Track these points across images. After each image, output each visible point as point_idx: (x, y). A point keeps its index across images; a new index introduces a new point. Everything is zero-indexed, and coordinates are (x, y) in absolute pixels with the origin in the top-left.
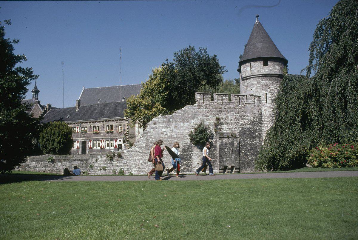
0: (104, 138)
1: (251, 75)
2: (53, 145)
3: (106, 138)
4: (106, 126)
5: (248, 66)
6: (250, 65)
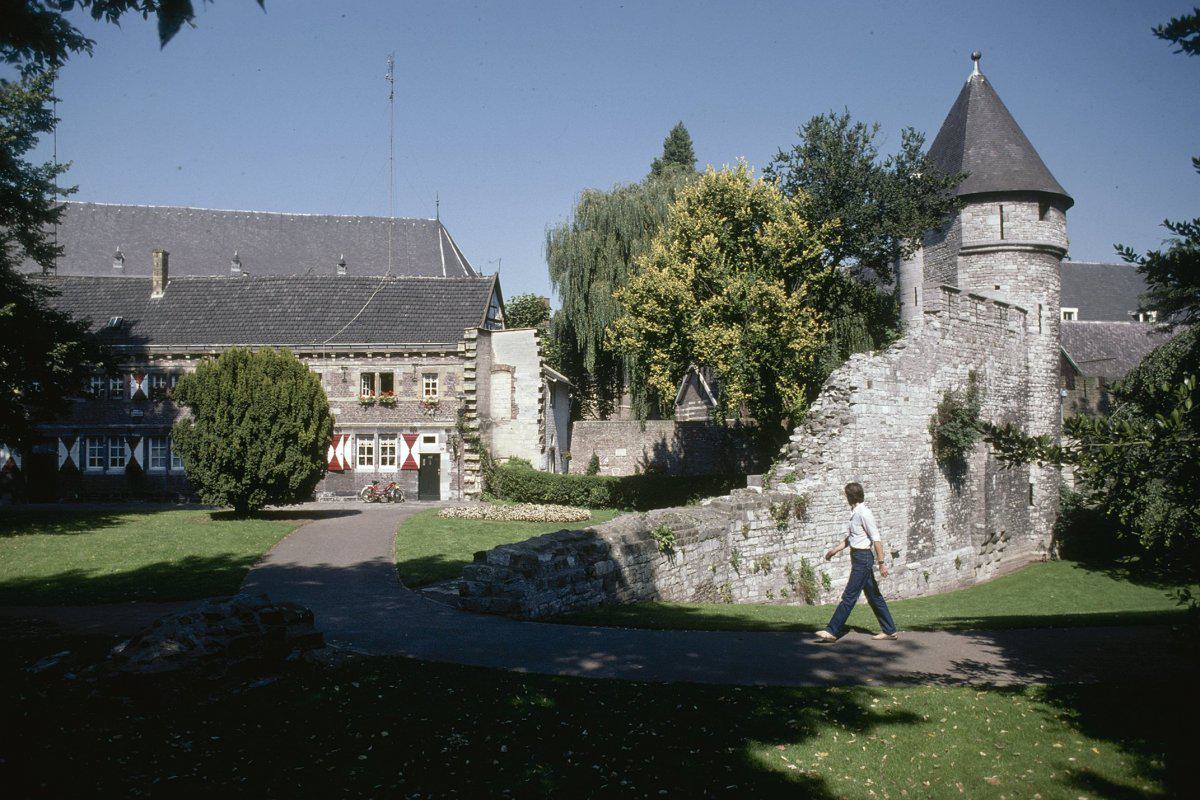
0: (350, 428)
1: (1003, 242)
2: (280, 459)
3: (357, 428)
4: (356, 376)
6: (999, 210)
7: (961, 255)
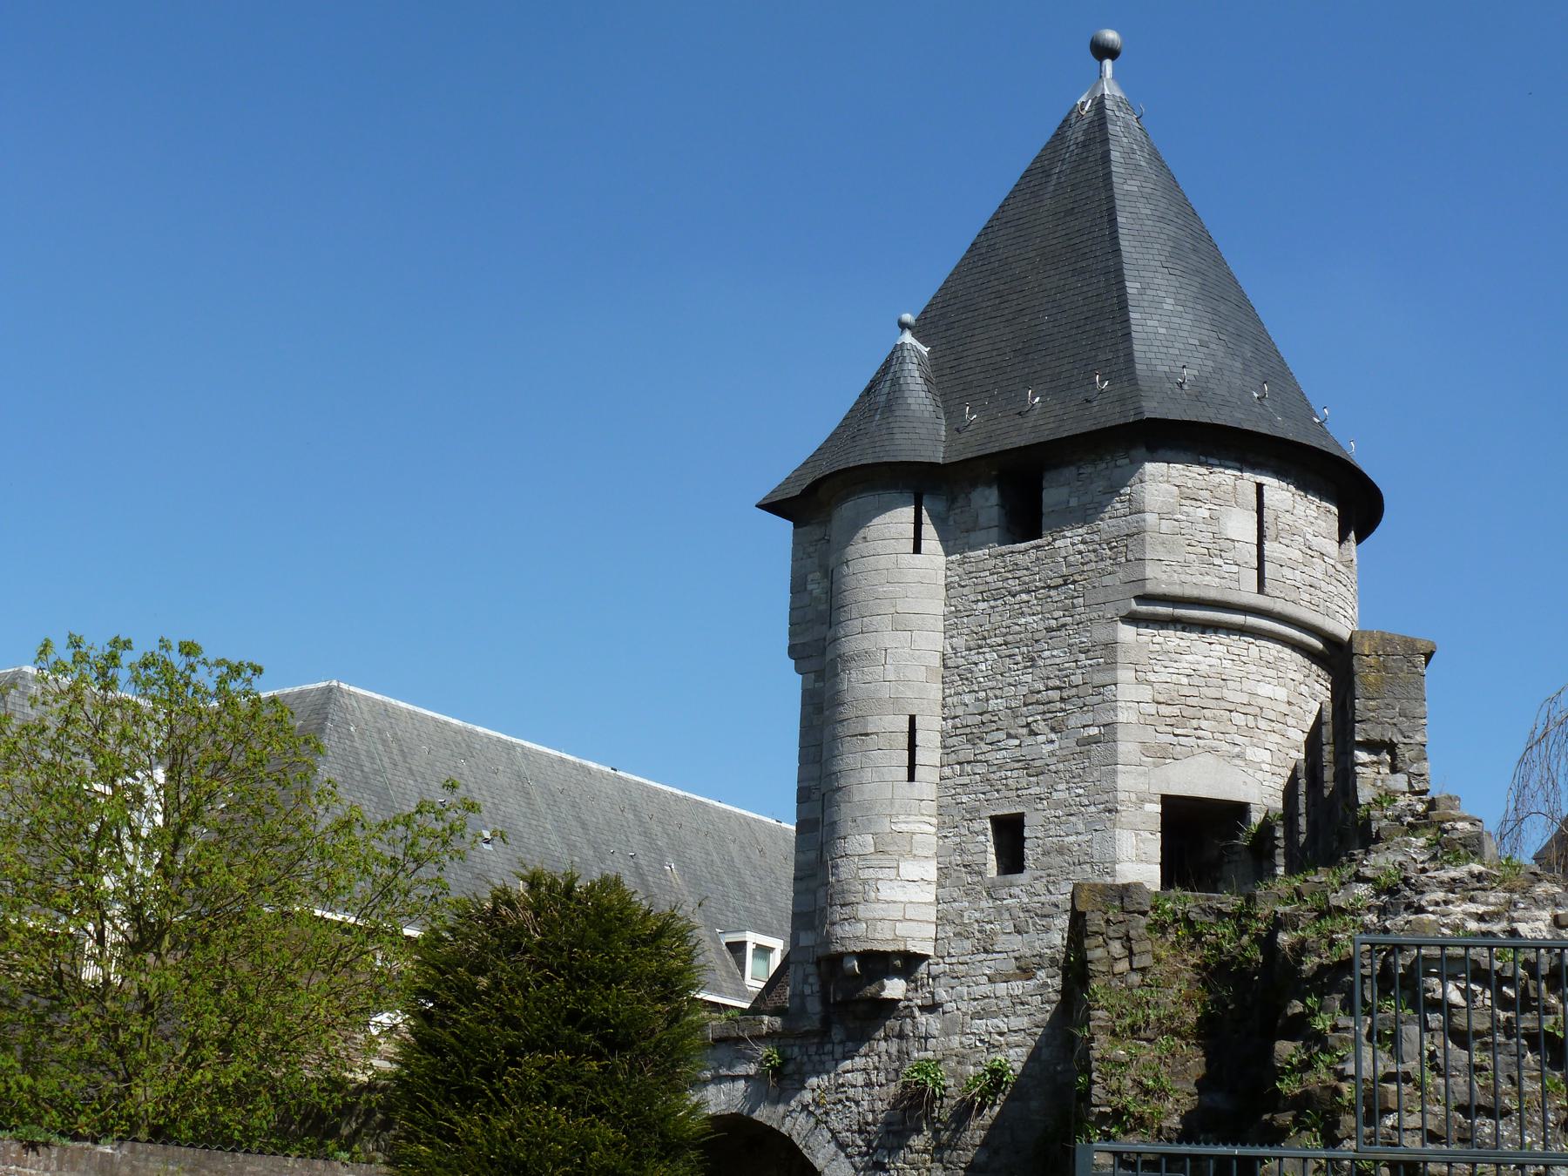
5: (1220, 500)
7: (1133, 619)
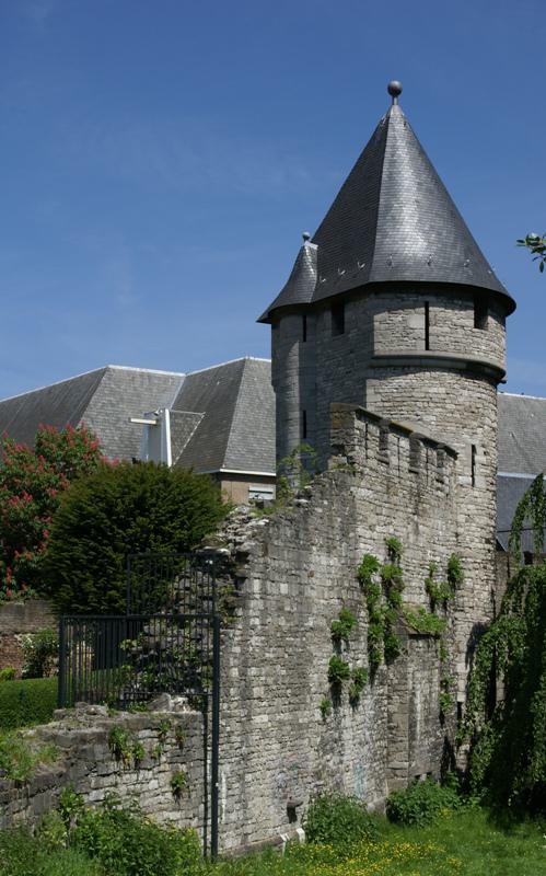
7: (372, 367)
